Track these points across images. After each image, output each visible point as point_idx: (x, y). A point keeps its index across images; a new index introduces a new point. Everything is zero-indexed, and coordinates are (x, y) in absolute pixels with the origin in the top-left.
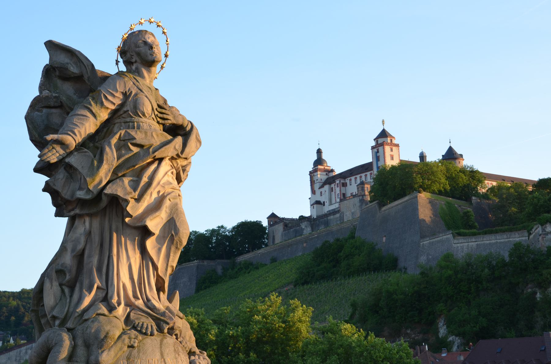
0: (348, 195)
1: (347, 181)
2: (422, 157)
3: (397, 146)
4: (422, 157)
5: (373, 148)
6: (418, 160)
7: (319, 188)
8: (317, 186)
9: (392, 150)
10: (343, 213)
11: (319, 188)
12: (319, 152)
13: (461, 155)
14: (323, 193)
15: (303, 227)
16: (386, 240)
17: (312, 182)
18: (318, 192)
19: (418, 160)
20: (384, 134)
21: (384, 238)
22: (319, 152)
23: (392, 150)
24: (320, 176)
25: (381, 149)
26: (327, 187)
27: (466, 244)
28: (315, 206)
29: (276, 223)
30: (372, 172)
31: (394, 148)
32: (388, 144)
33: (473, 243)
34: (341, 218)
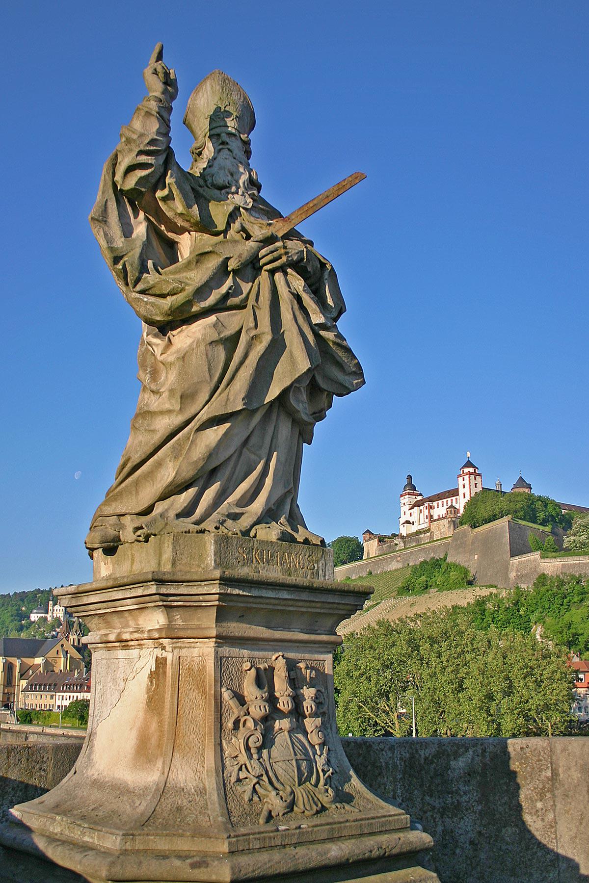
0: (435, 517)
1: (435, 504)
7: (409, 509)
10: (433, 532)
11: (409, 509)
12: (410, 477)
14: (412, 514)
16: (478, 558)
21: (476, 556)
22: (410, 477)
26: (416, 509)
27: (553, 564)
28: (405, 525)
30: (457, 497)
33: (558, 563)
34: (431, 536)
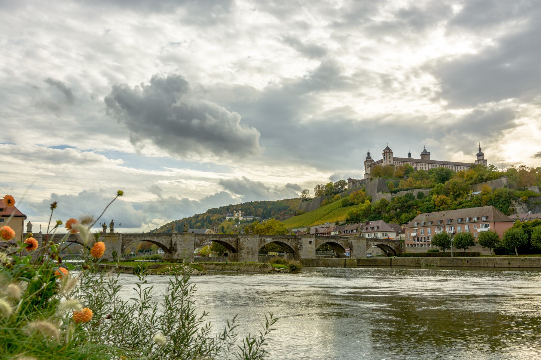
2: (410, 155)
3: (392, 153)
4: (410, 155)
5: (383, 154)
6: (407, 157)
8: (367, 167)
9: (390, 155)
12: (369, 153)
13: (429, 153)
15: (357, 184)
17: (365, 166)
18: (367, 169)
19: (407, 157)
20: (387, 148)
22: (369, 153)
23: (390, 155)
24: (369, 163)
25: (385, 154)
29: (350, 181)
31: (391, 154)
32: (388, 153)
